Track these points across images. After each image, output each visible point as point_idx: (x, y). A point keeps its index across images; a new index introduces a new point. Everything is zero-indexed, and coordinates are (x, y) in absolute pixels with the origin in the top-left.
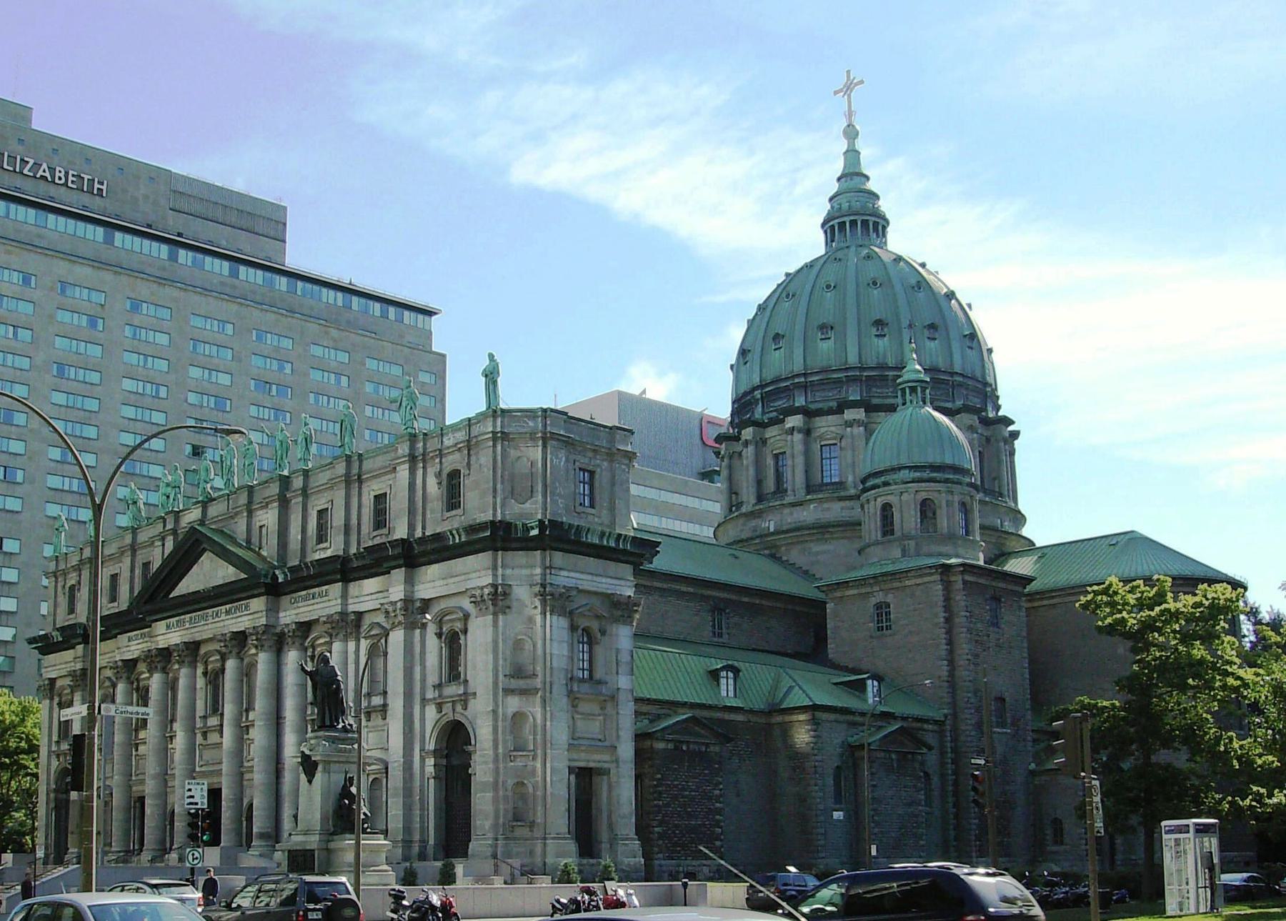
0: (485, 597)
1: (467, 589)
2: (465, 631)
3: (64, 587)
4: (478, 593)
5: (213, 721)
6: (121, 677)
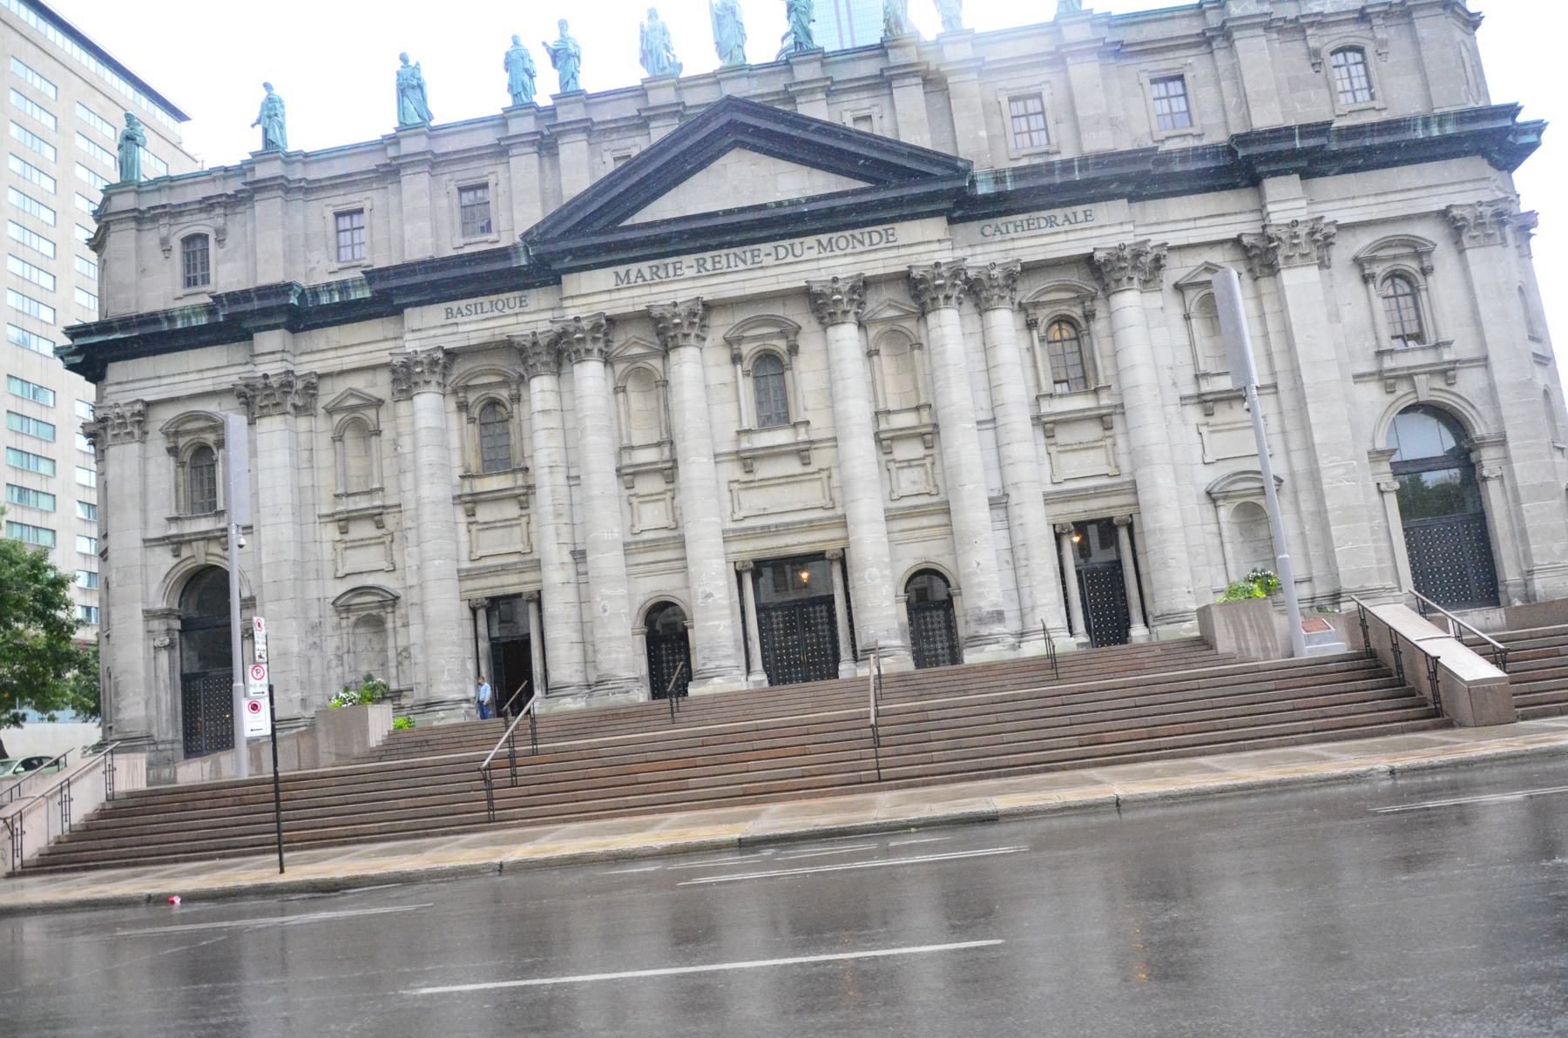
0: (1487, 220)
1: (1451, 206)
2: (1426, 272)
3: (164, 242)
4: (1467, 213)
5: (782, 437)
6: (427, 383)
